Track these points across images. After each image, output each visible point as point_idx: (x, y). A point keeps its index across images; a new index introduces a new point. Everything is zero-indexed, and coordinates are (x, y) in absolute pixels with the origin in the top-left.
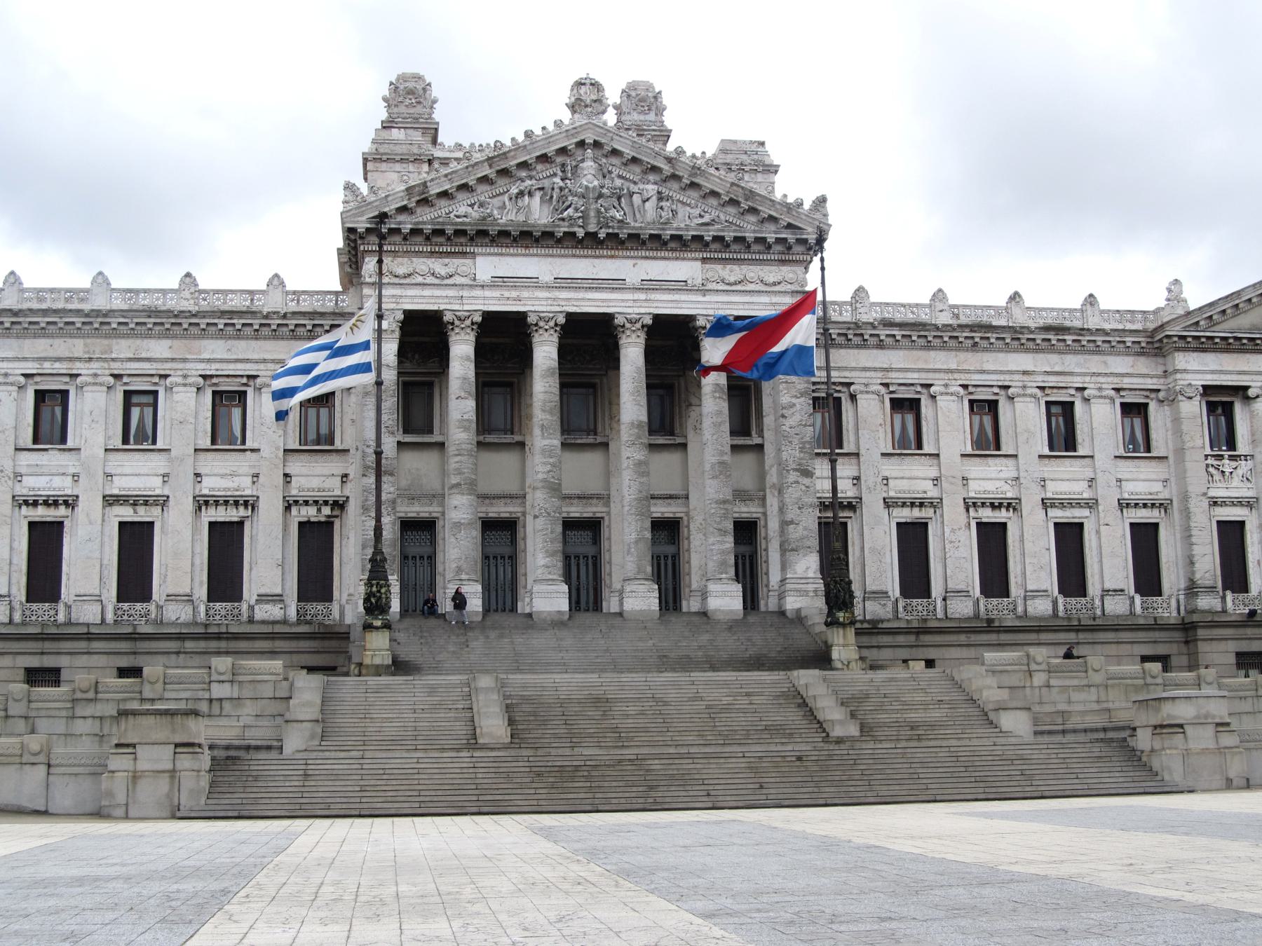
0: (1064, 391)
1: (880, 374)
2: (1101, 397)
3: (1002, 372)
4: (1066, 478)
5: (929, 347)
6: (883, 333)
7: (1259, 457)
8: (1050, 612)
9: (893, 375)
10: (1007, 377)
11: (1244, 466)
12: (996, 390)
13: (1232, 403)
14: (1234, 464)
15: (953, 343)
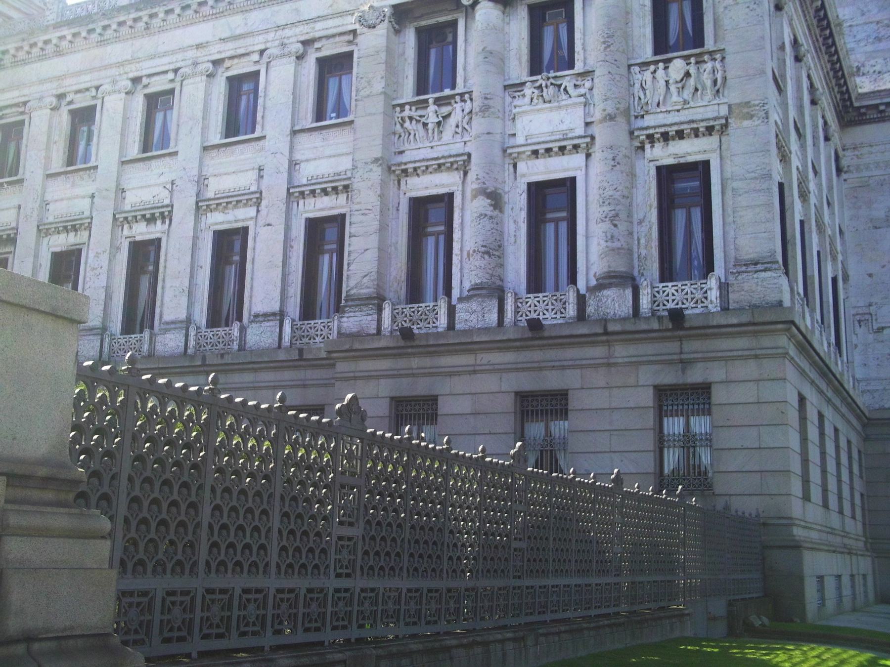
0: (246, 59)
1: (55, 84)
2: (283, 56)
3: (173, 52)
4: (232, 172)
5: (102, 43)
6: (53, 36)
7: (475, 95)
8: (182, 349)
9: (67, 82)
10: (180, 56)
11: (457, 112)
12: (171, 76)
13: (454, 24)
14: (445, 110)
15: (124, 30)
